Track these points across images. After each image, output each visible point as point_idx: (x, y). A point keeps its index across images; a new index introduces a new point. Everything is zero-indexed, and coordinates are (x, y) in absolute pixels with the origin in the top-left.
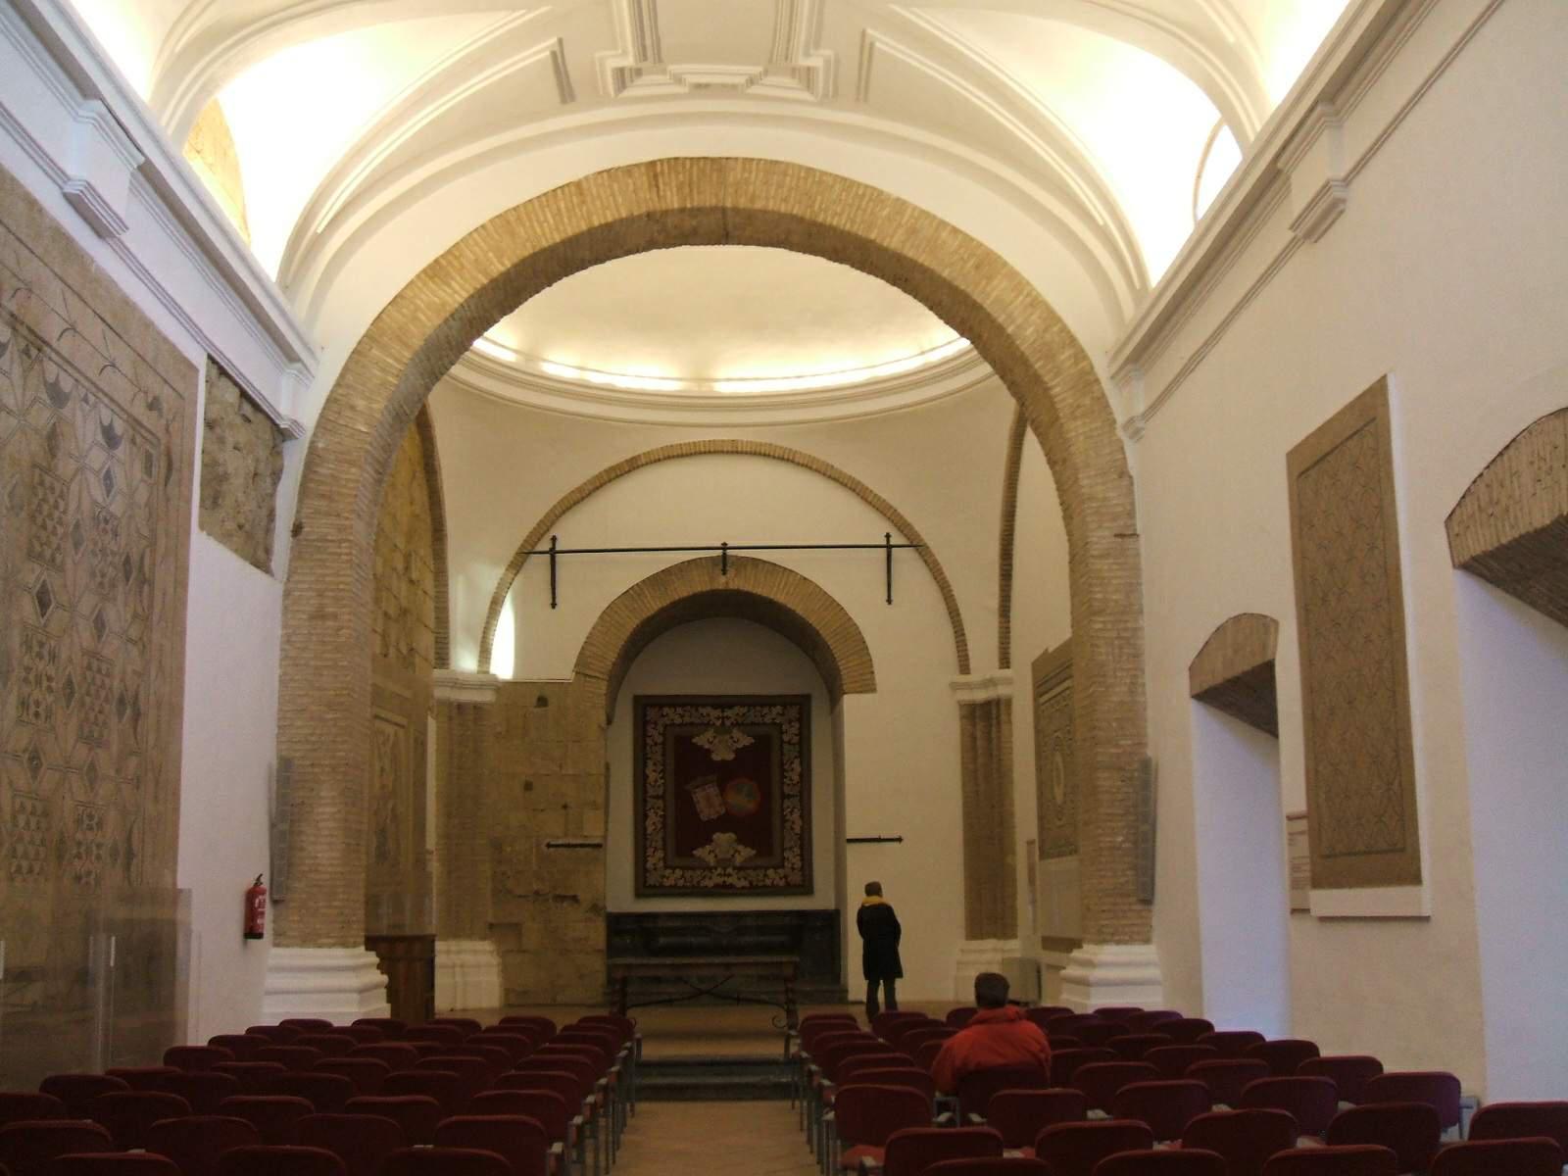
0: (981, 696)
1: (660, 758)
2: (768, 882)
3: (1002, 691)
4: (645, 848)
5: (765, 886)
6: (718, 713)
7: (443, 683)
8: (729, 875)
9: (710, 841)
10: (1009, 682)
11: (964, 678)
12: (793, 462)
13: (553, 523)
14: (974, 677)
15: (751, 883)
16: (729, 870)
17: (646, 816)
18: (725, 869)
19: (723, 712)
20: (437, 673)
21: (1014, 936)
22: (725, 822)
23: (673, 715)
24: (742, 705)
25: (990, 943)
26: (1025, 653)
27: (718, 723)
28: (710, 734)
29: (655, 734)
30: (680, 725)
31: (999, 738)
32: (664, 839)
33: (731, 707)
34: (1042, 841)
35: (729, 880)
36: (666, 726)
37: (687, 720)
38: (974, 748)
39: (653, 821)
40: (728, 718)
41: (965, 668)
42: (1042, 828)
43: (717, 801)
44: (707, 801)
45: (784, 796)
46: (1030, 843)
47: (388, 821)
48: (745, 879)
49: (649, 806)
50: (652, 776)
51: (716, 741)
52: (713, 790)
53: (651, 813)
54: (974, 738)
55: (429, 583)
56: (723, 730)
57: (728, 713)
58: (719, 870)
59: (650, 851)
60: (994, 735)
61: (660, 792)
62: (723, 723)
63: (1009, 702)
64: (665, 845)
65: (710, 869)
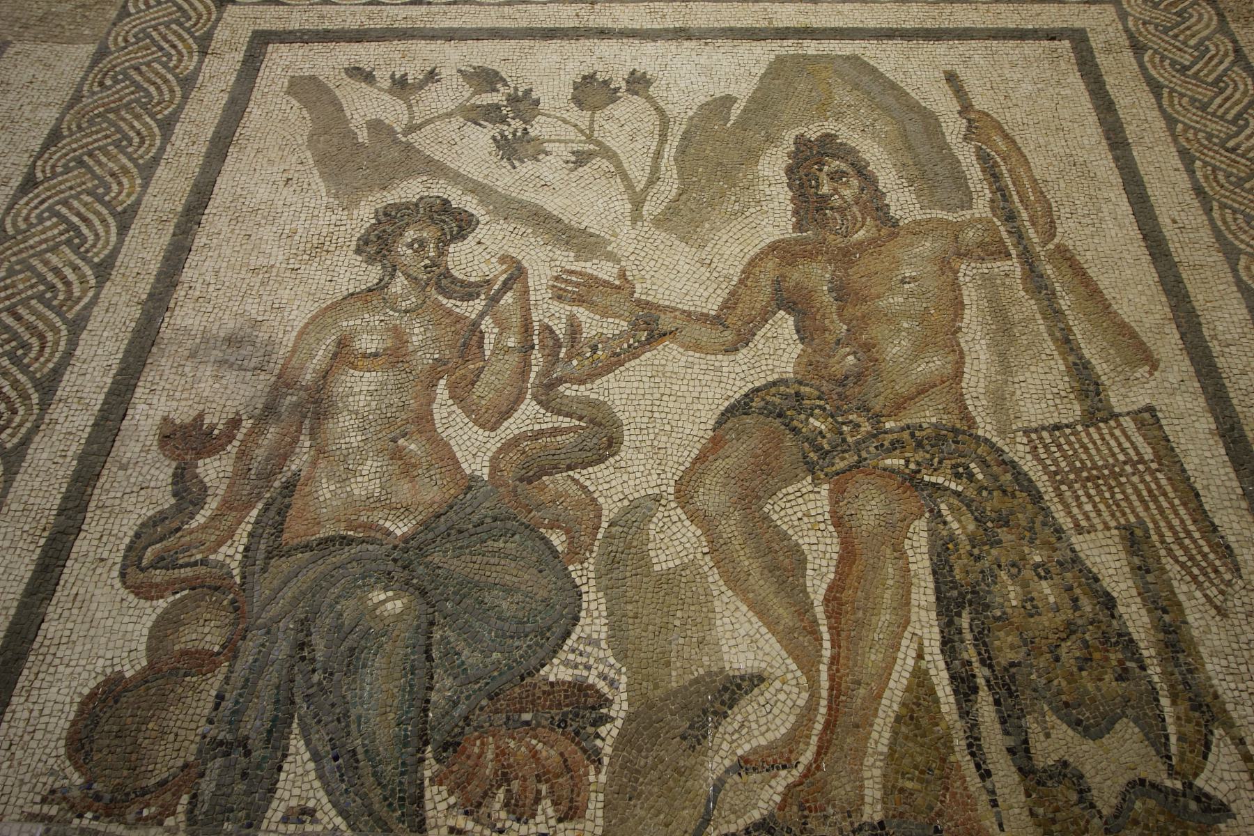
47: (612, 485)
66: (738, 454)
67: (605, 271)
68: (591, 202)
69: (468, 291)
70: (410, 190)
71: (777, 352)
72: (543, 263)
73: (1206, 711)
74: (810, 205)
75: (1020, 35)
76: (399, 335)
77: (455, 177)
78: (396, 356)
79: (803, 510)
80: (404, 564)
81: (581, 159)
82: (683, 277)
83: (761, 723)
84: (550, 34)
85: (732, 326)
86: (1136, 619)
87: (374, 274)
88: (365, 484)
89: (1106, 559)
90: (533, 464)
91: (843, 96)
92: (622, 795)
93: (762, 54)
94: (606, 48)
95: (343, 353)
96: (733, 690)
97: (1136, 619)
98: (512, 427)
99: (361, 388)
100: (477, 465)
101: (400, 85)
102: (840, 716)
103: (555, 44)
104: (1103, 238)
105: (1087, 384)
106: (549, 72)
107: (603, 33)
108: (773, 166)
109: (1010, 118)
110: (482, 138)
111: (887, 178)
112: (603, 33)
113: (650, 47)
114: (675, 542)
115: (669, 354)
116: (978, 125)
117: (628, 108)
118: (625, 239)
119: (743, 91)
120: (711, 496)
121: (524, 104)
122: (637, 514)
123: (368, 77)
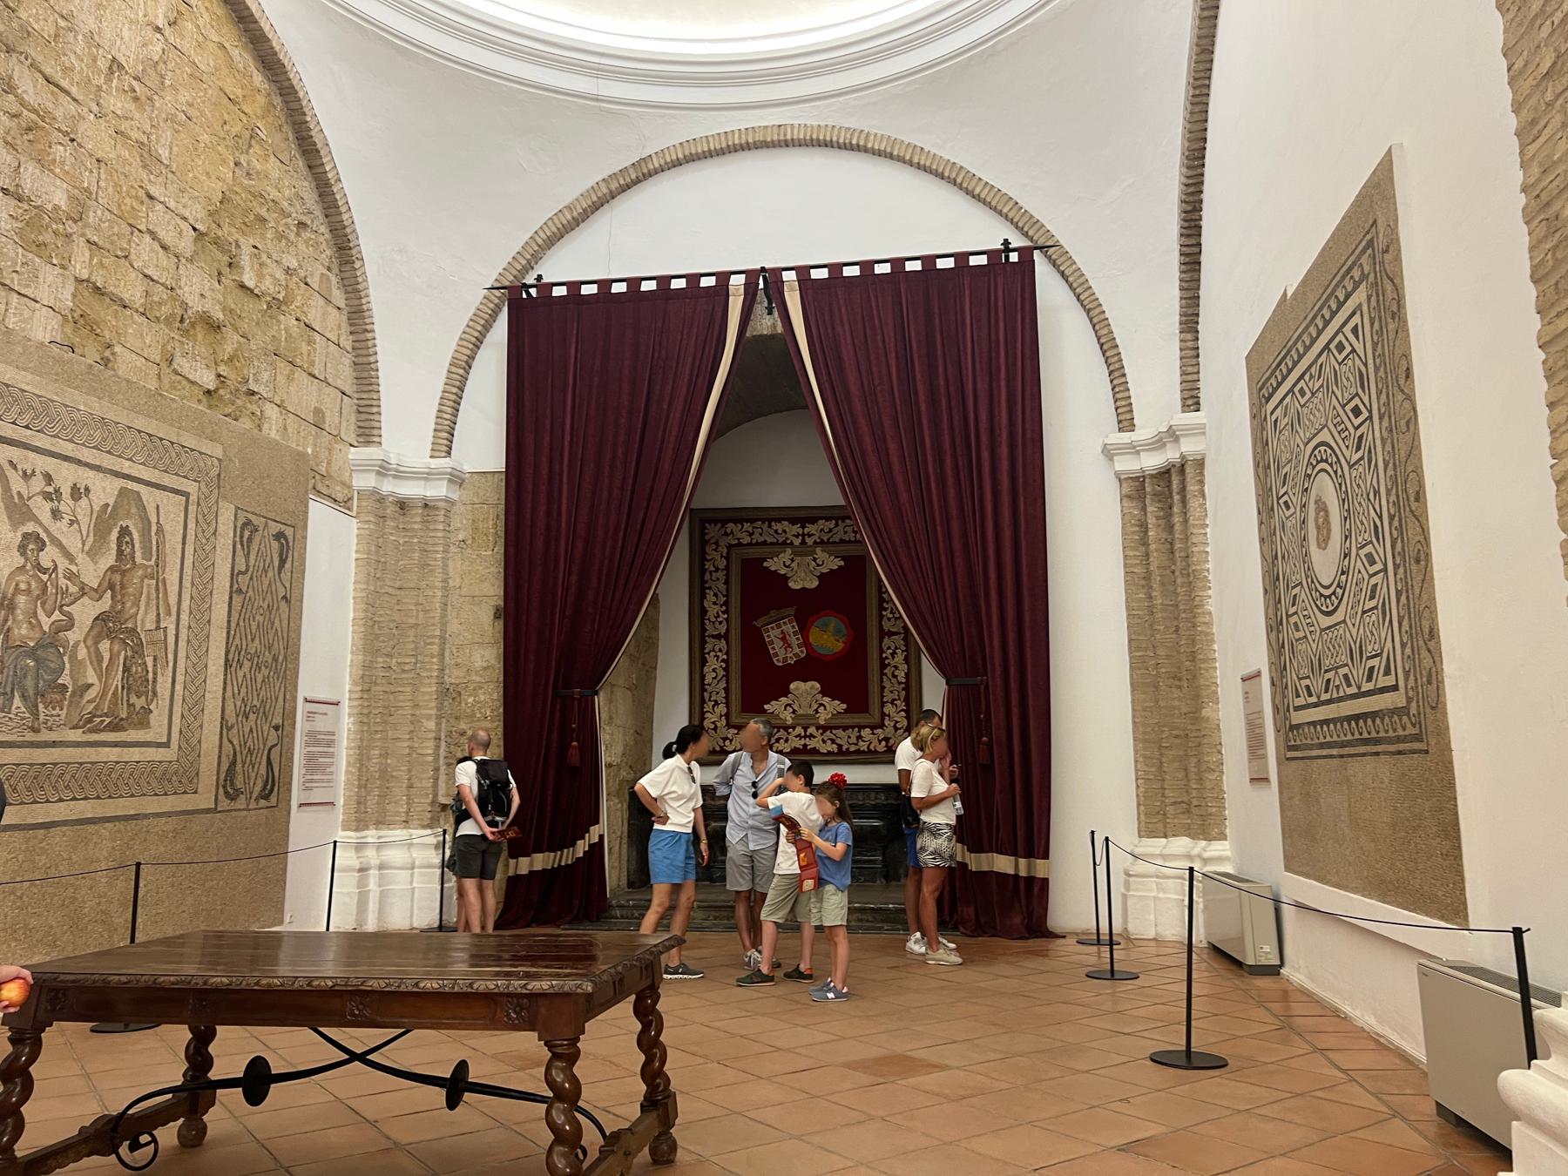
0: (1152, 461)
1: (722, 587)
2: (863, 746)
3: (1189, 447)
4: (703, 701)
5: (858, 752)
6: (796, 529)
7: (363, 468)
8: (811, 736)
9: (786, 693)
10: (1200, 430)
11: (1126, 437)
12: (866, 150)
13: (536, 258)
14: (1142, 433)
15: (840, 746)
16: (812, 730)
17: (704, 662)
18: (805, 729)
19: (803, 527)
20: (355, 454)
21: (1222, 837)
22: (807, 668)
23: (741, 533)
24: (828, 519)
25: (1181, 844)
26: (1238, 315)
27: (797, 542)
28: (786, 555)
29: (716, 558)
30: (750, 544)
31: (1186, 521)
32: (726, 690)
33: (813, 520)
34: (1279, 669)
35: (812, 744)
36: (730, 547)
37: (757, 538)
38: (1144, 542)
39: (713, 664)
40: (810, 535)
41: (1126, 422)
42: (1279, 649)
43: (794, 641)
44: (783, 641)
45: (883, 633)
46: (1251, 678)
47: (73, 636)
48: (833, 742)
49: (708, 647)
50: (712, 610)
51: (794, 565)
52: (790, 627)
53: (711, 658)
54: (1143, 527)
55: (329, 319)
56: (803, 550)
57: (810, 528)
58: (799, 730)
59: (708, 706)
60: (1177, 519)
61: (723, 629)
62: (803, 542)
63: (1200, 464)
64: (727, 698)
65: (786, 728)
66: (96, 630)
67: (74, 569)
68: (74, 544)
69: (44, 571)
70: (30, 527)
71: (106, 603)
72: (62, 564)
73: (155, 694)
74: (120, 552)
75: (176, 492)
76: (29, 583)
77: (41, 524)
78: (28, 591)
79: (105, 646)
80: (32, 653)
81: (72, 523)
82: (92, 574)
83: (91, 694)
84: (66, 458)
85: (98, 594)
86: (150, 676)
87: (22, 561)
88: (24, 632)
89: (150, 661)
90: (59, 628)
91: (133, 510)
92: (69, 705)
93: (120, 483)
94: (81, 470)
95: (17, 590)
96: (90, 686)
97: (150, 676)
98: (54, 618)
99: (21, 600)
100: (46, 628)
101: (25, 472)
102: (104, 693)
103: (66, 464)
104: (172, 578)
105: (158, 621)
106: (66, 476)
107: (79, 462)
108: (114, 535)
109: (166, 527)
110: (47, 506)
111: (137, 546)
112: (79, 462)
113: (92, 473)
114: (82, 653)
115: (85, 599)
116: (160, 530)
117: (84, 502)
118: (81, 558)
119: (111, 502)
120: (90, 642)
121: (57, 491)
122: (77, 644)
123: (15, 468)
